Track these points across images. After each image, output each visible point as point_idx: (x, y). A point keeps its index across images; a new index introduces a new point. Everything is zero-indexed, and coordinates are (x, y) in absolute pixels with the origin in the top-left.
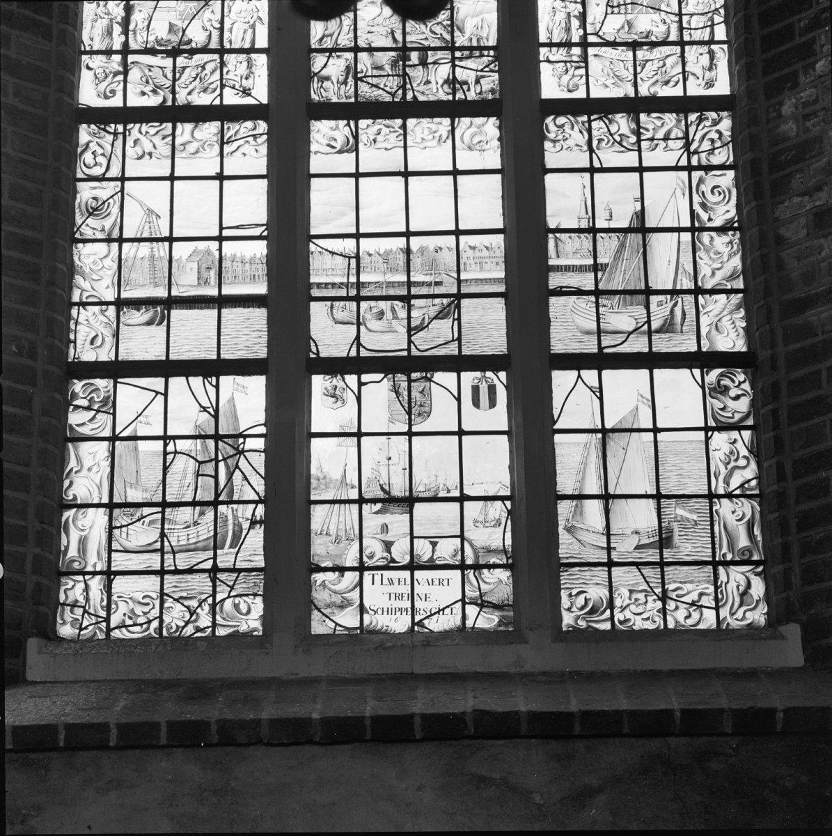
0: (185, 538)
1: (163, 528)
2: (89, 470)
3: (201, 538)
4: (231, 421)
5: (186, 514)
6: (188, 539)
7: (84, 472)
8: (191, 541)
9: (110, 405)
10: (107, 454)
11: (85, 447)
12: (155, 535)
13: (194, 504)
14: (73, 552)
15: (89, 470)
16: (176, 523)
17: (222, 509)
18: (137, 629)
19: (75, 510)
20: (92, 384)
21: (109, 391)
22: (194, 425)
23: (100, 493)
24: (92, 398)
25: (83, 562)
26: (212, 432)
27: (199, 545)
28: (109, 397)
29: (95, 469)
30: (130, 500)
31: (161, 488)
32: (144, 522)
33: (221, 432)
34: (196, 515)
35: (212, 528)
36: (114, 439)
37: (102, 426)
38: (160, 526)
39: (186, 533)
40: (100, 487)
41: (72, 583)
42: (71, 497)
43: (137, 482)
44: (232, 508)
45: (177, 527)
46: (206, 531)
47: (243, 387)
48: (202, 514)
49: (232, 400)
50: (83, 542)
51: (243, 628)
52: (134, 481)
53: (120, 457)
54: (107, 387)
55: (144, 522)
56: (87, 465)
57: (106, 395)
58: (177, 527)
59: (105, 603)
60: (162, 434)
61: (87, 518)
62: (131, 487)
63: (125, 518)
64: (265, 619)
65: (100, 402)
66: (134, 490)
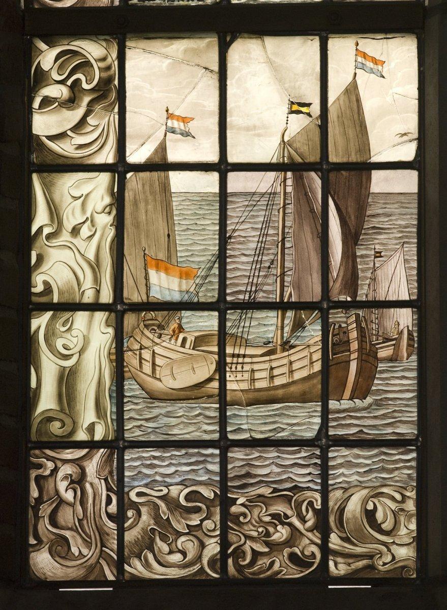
0: (265, 374)
1: (222, 354)
2: (75, 231)
3: (297, 376)
4: (351, 133)
5: (267, 325)
6: (272, 378)
7: (65, 237)
8: (278, 382)
9: (112, 92)
10: (108, 200)
11: (69, 185)
12: (205, 369)
13: (281, 306)
14: (47, 402)
15: (75, 231)
16: (247, 344)
17: (337, 317)
18: (177, 558)
19: (49, 314)
20: (75, 53)
21: (109, 68)
22: (279, 140)
23: (97, 280)
24: (78, 81)
25: (68, 421)
26: (314, 157)
27: (293, 389)
28: (110, 80)
29: (85, 231)
30: (157, 294)
31: (216, 271)
32: (185, 340)
33: (333, 158)
34: (287, 329)
35: (317, 356)
36: (120, 168)
37: (96, 140)
38: (216, 349)
39: (267, 366)
40: (95, 267)
41: (50, 465)
42: (39, 288)
43: (169, 257)
44: (357, 316)
45: (249, 351)
46: (306, 362)
47: (375, 61)
48: (298, 325)
49: (352, 90)
50: (67, 381)
51: (383, 564)
52: (162, 255)
53: (136, 203)
54: (104, 59)
55: (185, 340)
56: (69, 224)
57: (104, 75)
58: (249, 351)
59: (113, 508)
60: (213, 156)
61: (74, 333)
62: (158, 268)
63: (147, 332)
64: (421, 540)
65: (93, 90)
66: (163, 275)
